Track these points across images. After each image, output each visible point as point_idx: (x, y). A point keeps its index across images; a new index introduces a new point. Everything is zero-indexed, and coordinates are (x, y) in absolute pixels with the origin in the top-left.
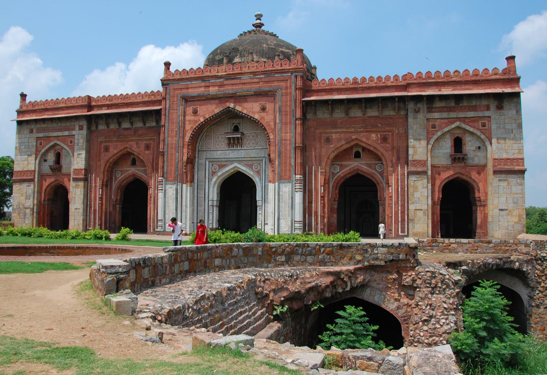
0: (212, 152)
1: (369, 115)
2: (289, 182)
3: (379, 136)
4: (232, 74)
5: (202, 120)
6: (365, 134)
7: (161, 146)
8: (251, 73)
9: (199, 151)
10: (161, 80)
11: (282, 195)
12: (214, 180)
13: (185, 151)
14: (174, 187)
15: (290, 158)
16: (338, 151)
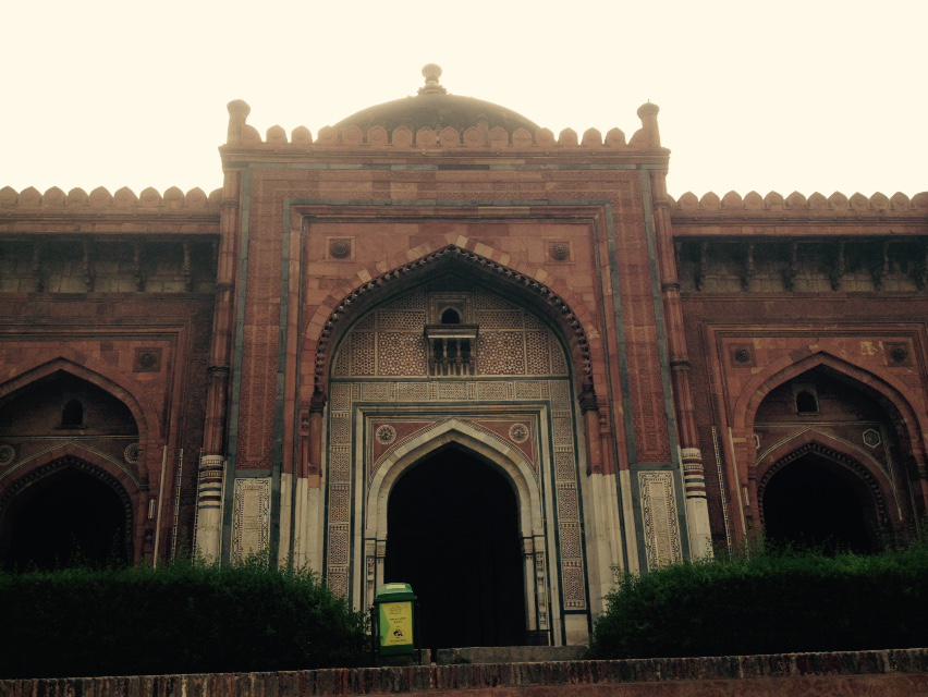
0: (377, 386)
1: (850, 290)
2: (665, 468)
3: (881, 345)
4: (462, 154)
5: (365, 277)
6: (844, 339)
7: (218, 352)
8: (519, 155)
9: (331, 381)
10: (220, 148)
11: (647, 510)
12: (382, 471)
13: (308, 369)
14: (267, 485)
15: (660, 395)
16: (773, 386)
